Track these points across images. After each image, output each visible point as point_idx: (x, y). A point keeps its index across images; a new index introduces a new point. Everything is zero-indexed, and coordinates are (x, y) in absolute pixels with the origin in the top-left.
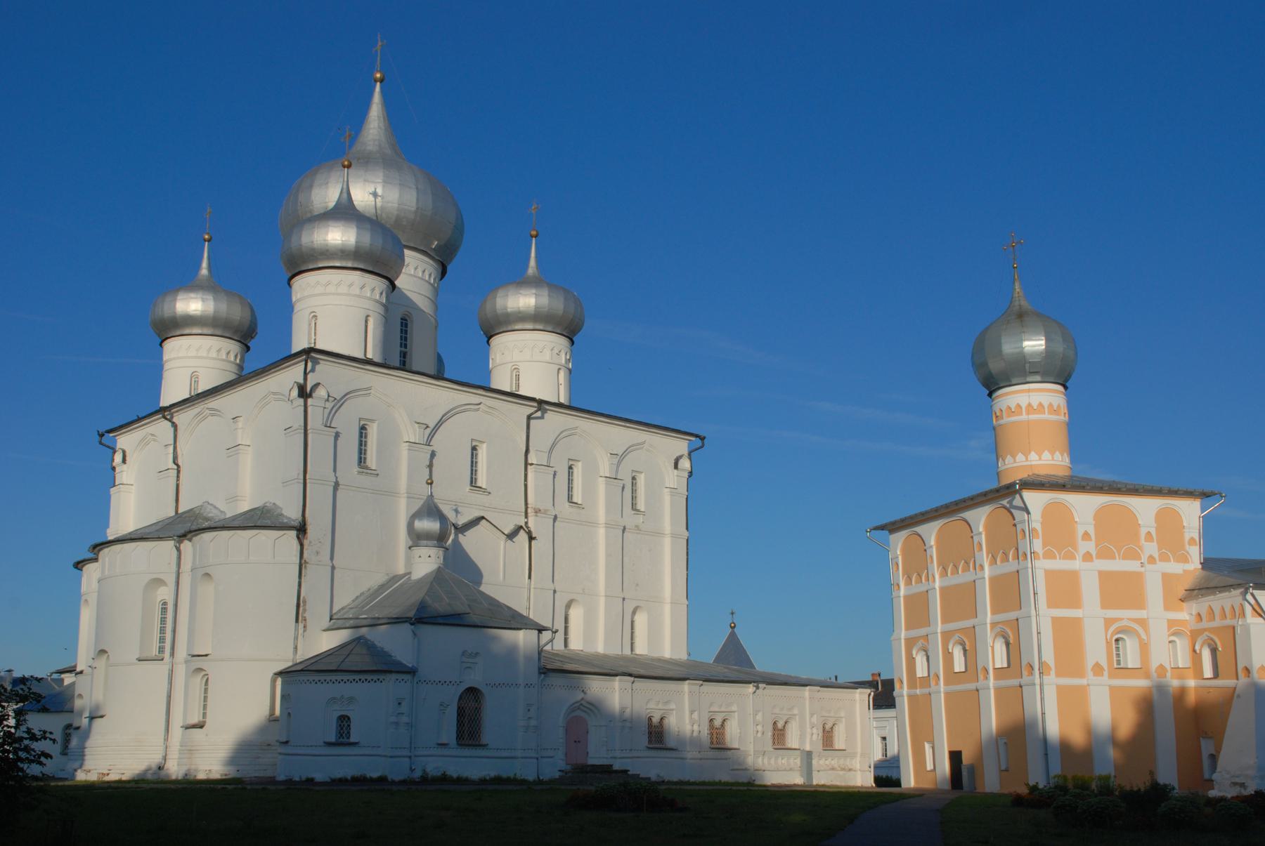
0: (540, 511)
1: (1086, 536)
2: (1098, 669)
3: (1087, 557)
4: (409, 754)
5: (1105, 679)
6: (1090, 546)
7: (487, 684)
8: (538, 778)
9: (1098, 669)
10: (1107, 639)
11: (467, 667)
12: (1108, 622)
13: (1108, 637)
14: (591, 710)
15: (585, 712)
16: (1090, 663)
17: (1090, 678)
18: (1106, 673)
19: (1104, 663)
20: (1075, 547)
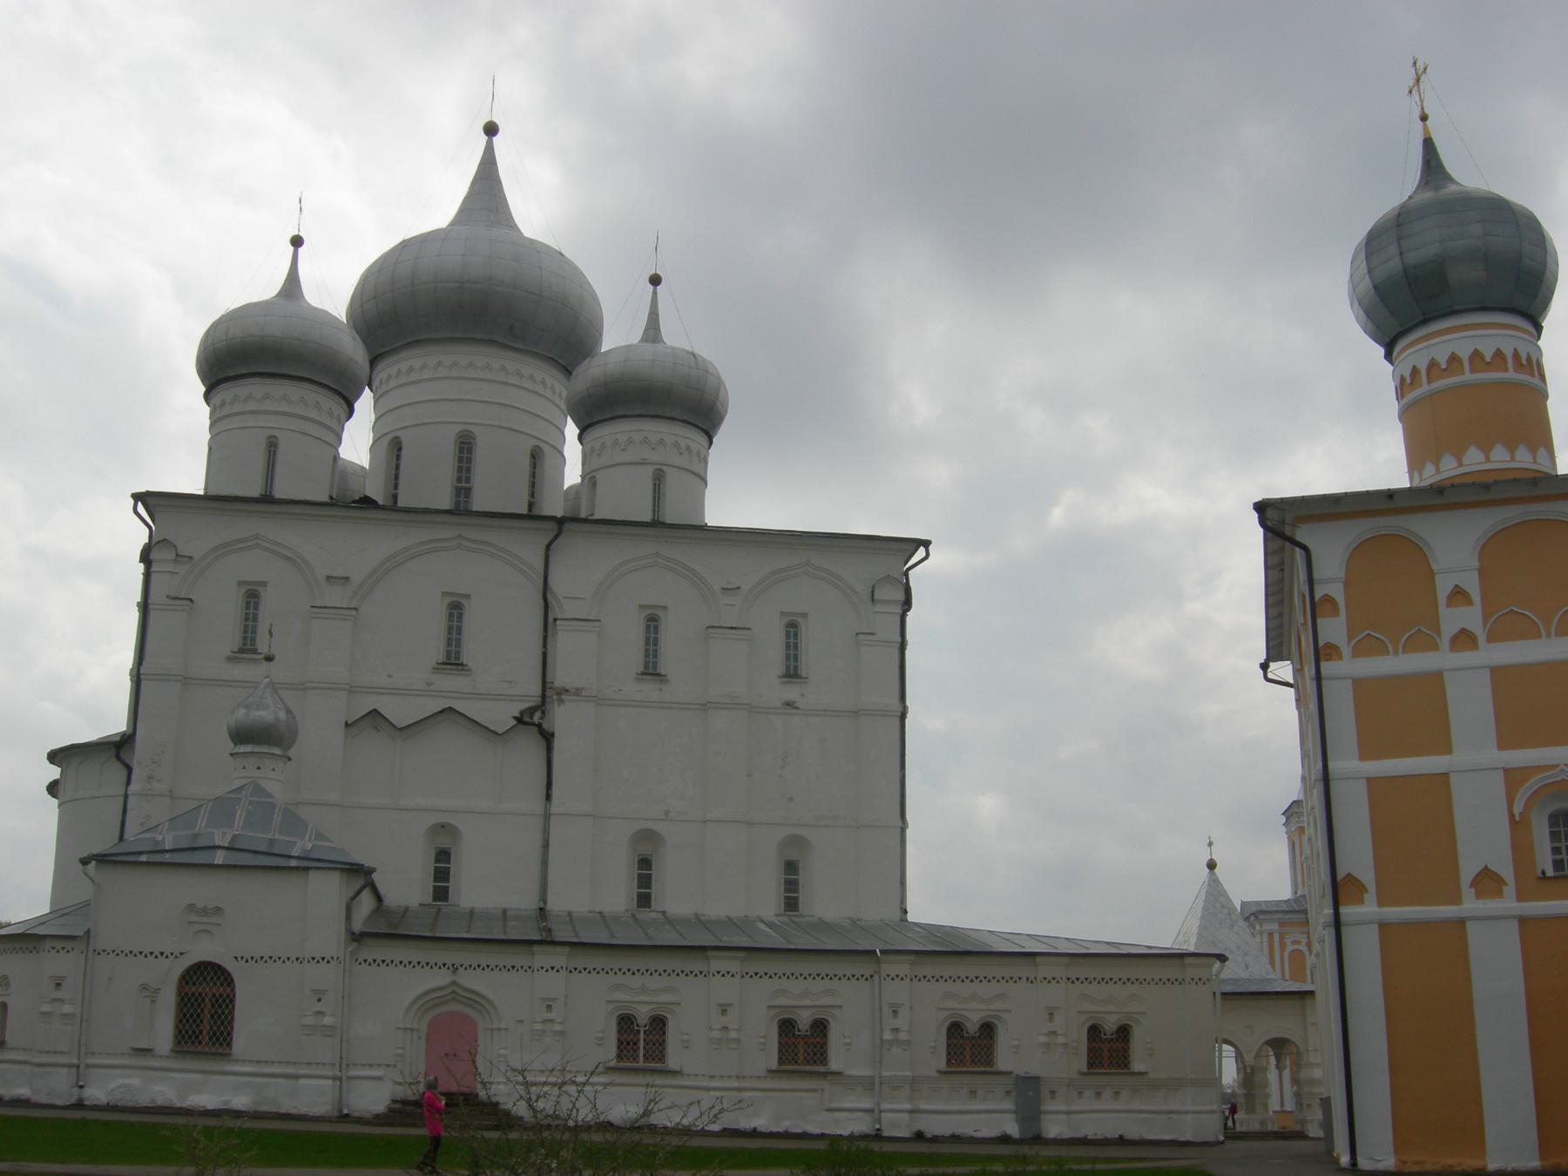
0: (567, 691)
1: (1459, 595)
2: (1487, 882)
3: (1464, 640)
4: (75, 1061)
5: (1508, 903)
6: (1470, 618)
7: (236, 958)
8: (340, 1110)
9: (1487, 882)
10: (1511, 816)
11: (199, 931)
12: (1513, 777)
13: (1517, 810)
14: (480, 1004)
15: (470, 1006)
16: (1468, 872)
17: (1471, 905)
18: (1510, 889)
19: (1505, 869)
20: (1436, 628)
